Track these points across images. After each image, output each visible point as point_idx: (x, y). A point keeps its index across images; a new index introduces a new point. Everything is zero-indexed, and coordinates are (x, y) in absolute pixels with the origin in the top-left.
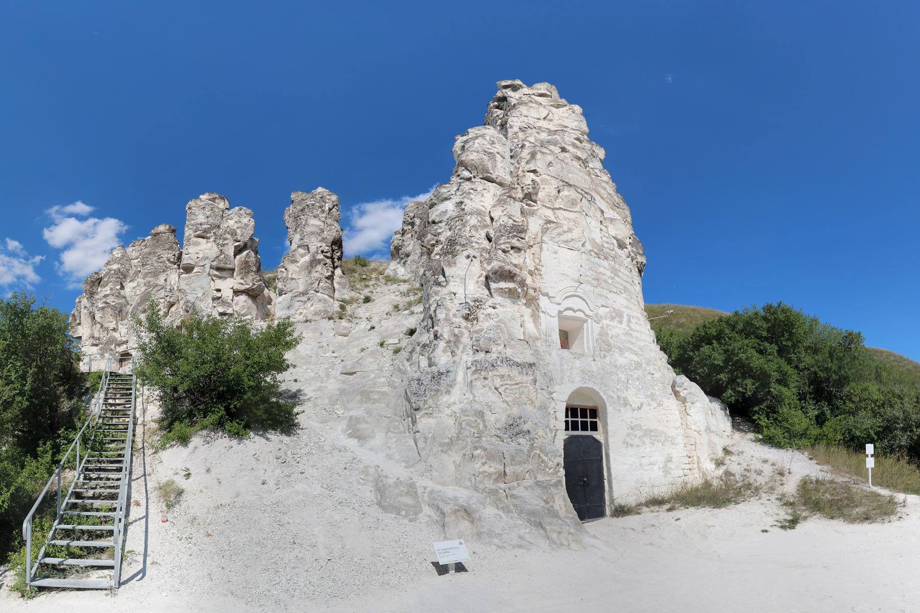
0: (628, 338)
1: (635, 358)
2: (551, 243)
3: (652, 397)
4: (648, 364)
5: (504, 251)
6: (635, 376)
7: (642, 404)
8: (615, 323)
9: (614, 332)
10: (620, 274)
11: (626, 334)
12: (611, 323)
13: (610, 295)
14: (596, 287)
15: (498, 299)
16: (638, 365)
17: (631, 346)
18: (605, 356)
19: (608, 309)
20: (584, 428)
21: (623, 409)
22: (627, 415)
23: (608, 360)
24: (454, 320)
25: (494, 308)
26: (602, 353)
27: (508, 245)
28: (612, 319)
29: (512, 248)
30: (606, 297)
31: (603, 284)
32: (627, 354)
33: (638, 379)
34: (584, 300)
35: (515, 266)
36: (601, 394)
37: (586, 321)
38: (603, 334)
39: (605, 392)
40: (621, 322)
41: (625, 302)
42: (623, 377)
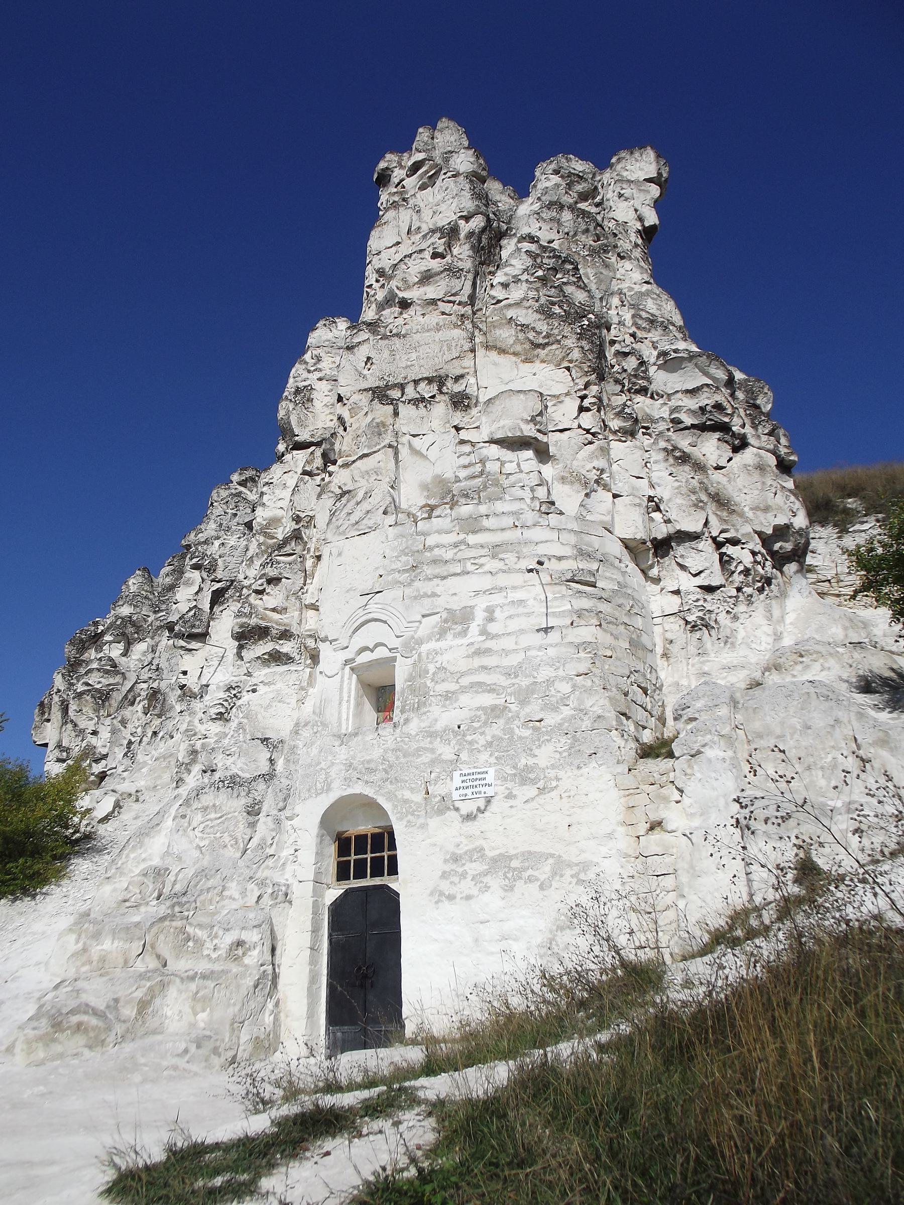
0: (477, 662)
1: (488, 700)
2: (337, 538)
3: (524, 776)
4: (523, 702)
5: (258, 592)
6: (482, 741)
7: (489, 801)
8: (449, 640)
9: (444, 659)
10: (486, 523)
11: (479, 653)
12: (442, 644)
13: (439, 587)
14: (410, 584)
15: (262, 673)
16: (496, 712)
17: (482, 677)
18: (407, 721)
19: (436, 618)
20: (377, 871)
21: (434, 822)
22: (447, 832)
23: (414, 726)
24: (201, 729)
25: (254, 691)
26: (405, 716)
27: (260, 582)
28: (442, 633)
29: (270, 581)
30: (434, 595)
31: (429, 571)
32: (465, 699)
33: (490, 744)
34: (385, 622)
35: (274, 610)
36: (381, 801)
37: (394, 659)
38: (418, 672)
39: (390, 796)
40: (464, 633)
41: (486, 582)
42: (447, 752)
